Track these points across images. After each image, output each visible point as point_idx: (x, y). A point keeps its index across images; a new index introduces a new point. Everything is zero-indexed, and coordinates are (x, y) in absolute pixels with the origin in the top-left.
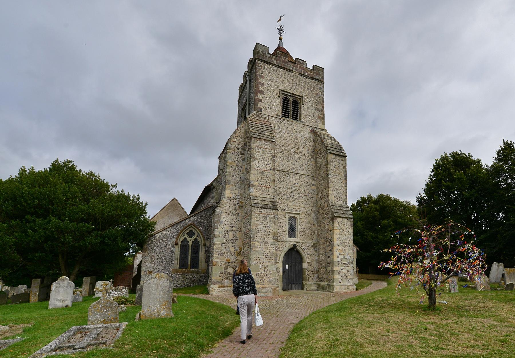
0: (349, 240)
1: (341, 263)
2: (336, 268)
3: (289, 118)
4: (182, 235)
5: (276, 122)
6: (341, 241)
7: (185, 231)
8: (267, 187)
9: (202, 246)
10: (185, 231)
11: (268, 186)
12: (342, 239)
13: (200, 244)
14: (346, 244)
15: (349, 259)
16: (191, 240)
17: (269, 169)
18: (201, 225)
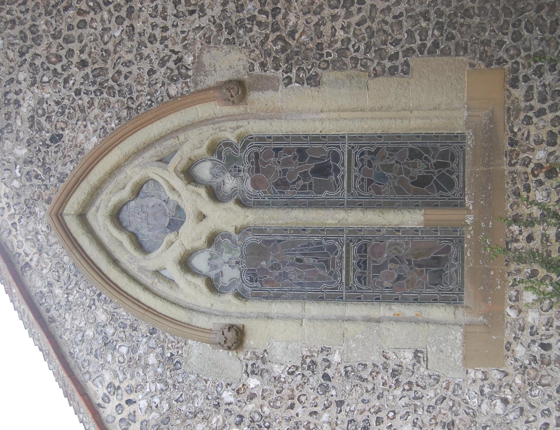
4: (161, 287)
7: (124, 271)
9: (244, 117)
10: (124, 271)
13: (232, 137)
16: (202, 217)
18: (56, 138)
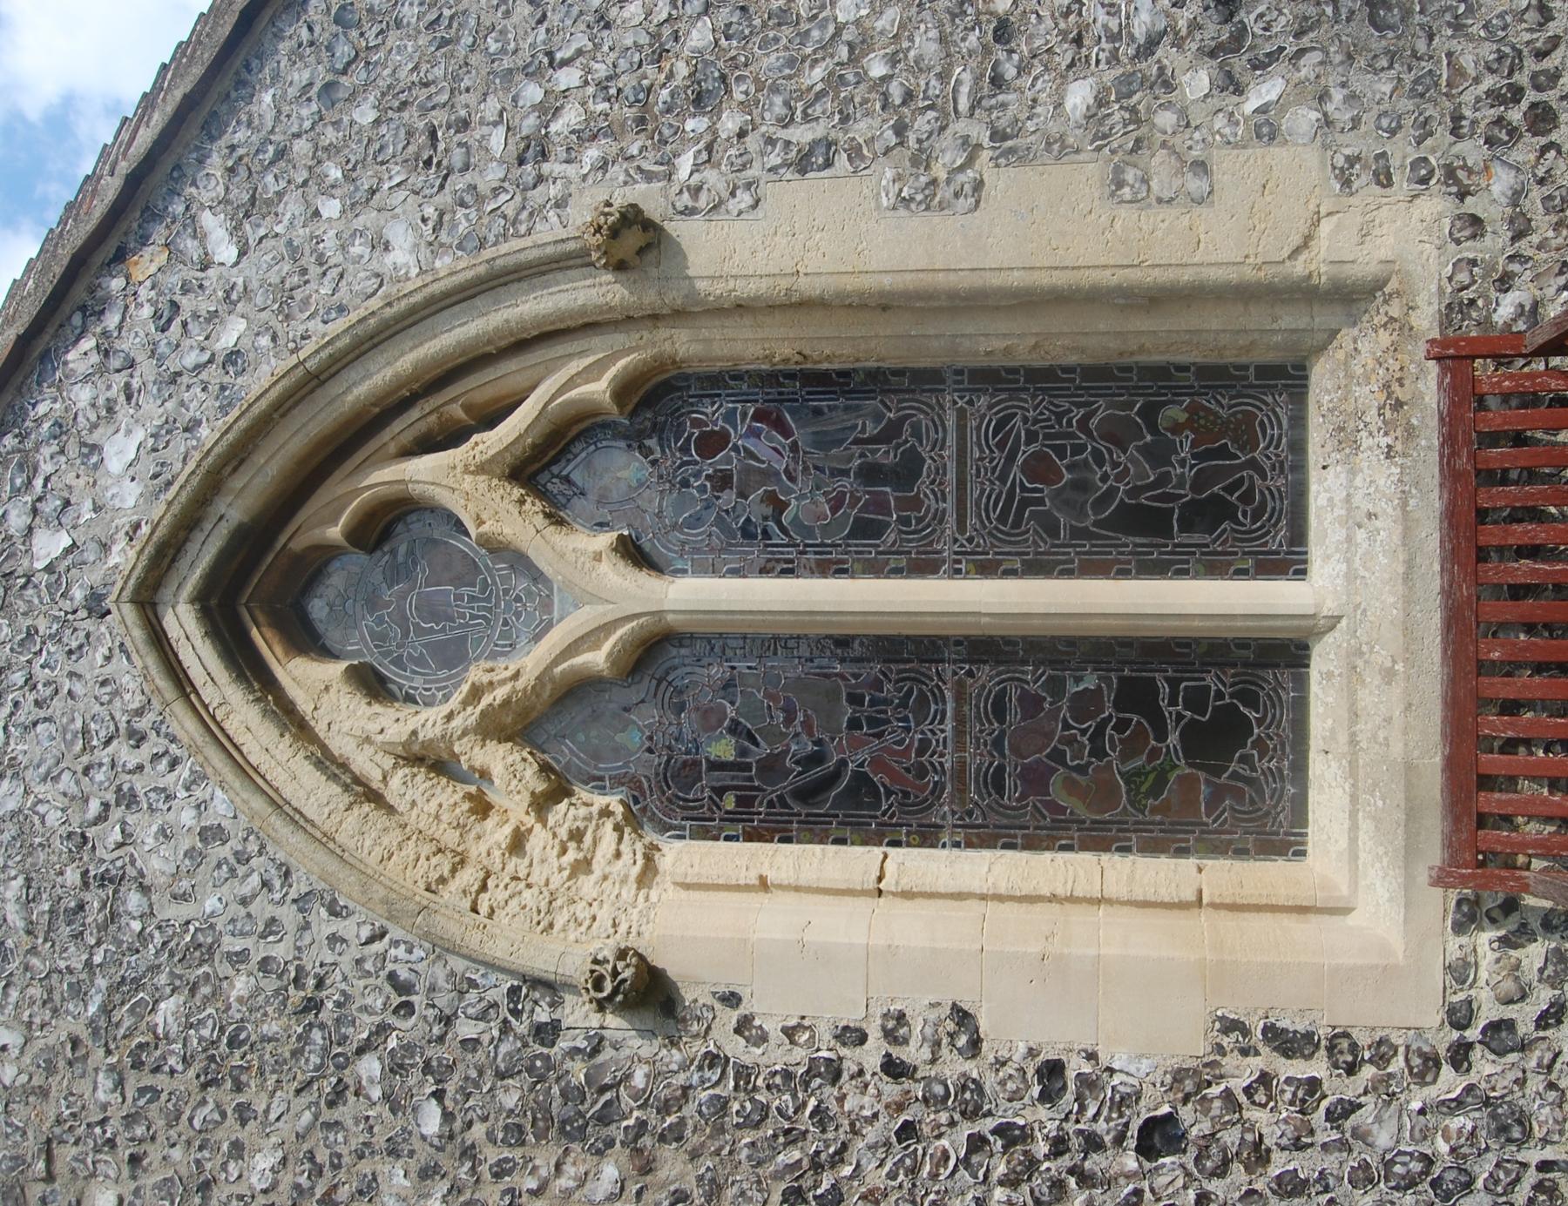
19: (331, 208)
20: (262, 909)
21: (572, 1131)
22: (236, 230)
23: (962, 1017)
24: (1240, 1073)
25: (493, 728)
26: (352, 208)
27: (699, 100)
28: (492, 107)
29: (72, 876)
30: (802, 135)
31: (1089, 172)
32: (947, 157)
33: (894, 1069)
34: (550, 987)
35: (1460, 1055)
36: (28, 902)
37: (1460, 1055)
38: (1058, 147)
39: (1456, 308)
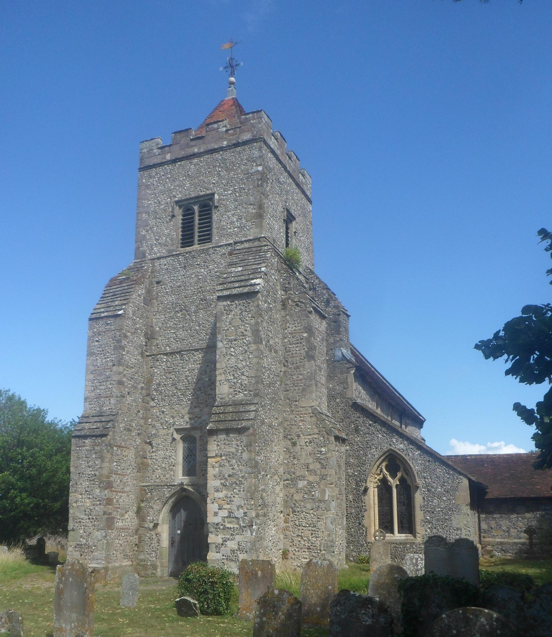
0: (243, 477)
1: (222, 527)
2: (212, 538)
3: (192, 245)
5: (165, 265)
6: (223, 481)
8: (107, 397)
11: (109, 395)
12: (226, 476)
14: (234, 485)
15: (242, 518)
17: (111, 364)
19: (420, 462)
20: (369, 460)
21: (356, 483)
22: (419, 454)
23: (366, 511)
24: (364, 529)
25: (384, 475)
26: (421, 464)
27: (428, 490)
28: (428, 474)
29: (371, 444)
30: (426, 498)
31: (423, 518)
32: (424, 508)
33: (363, 506)
34: (366, 482)
35: (366, 543)
36: (368, 440)
37: (366, 543)
38: (425, 516)
39: (414, 543)
